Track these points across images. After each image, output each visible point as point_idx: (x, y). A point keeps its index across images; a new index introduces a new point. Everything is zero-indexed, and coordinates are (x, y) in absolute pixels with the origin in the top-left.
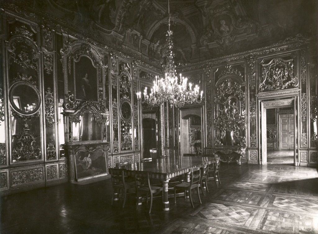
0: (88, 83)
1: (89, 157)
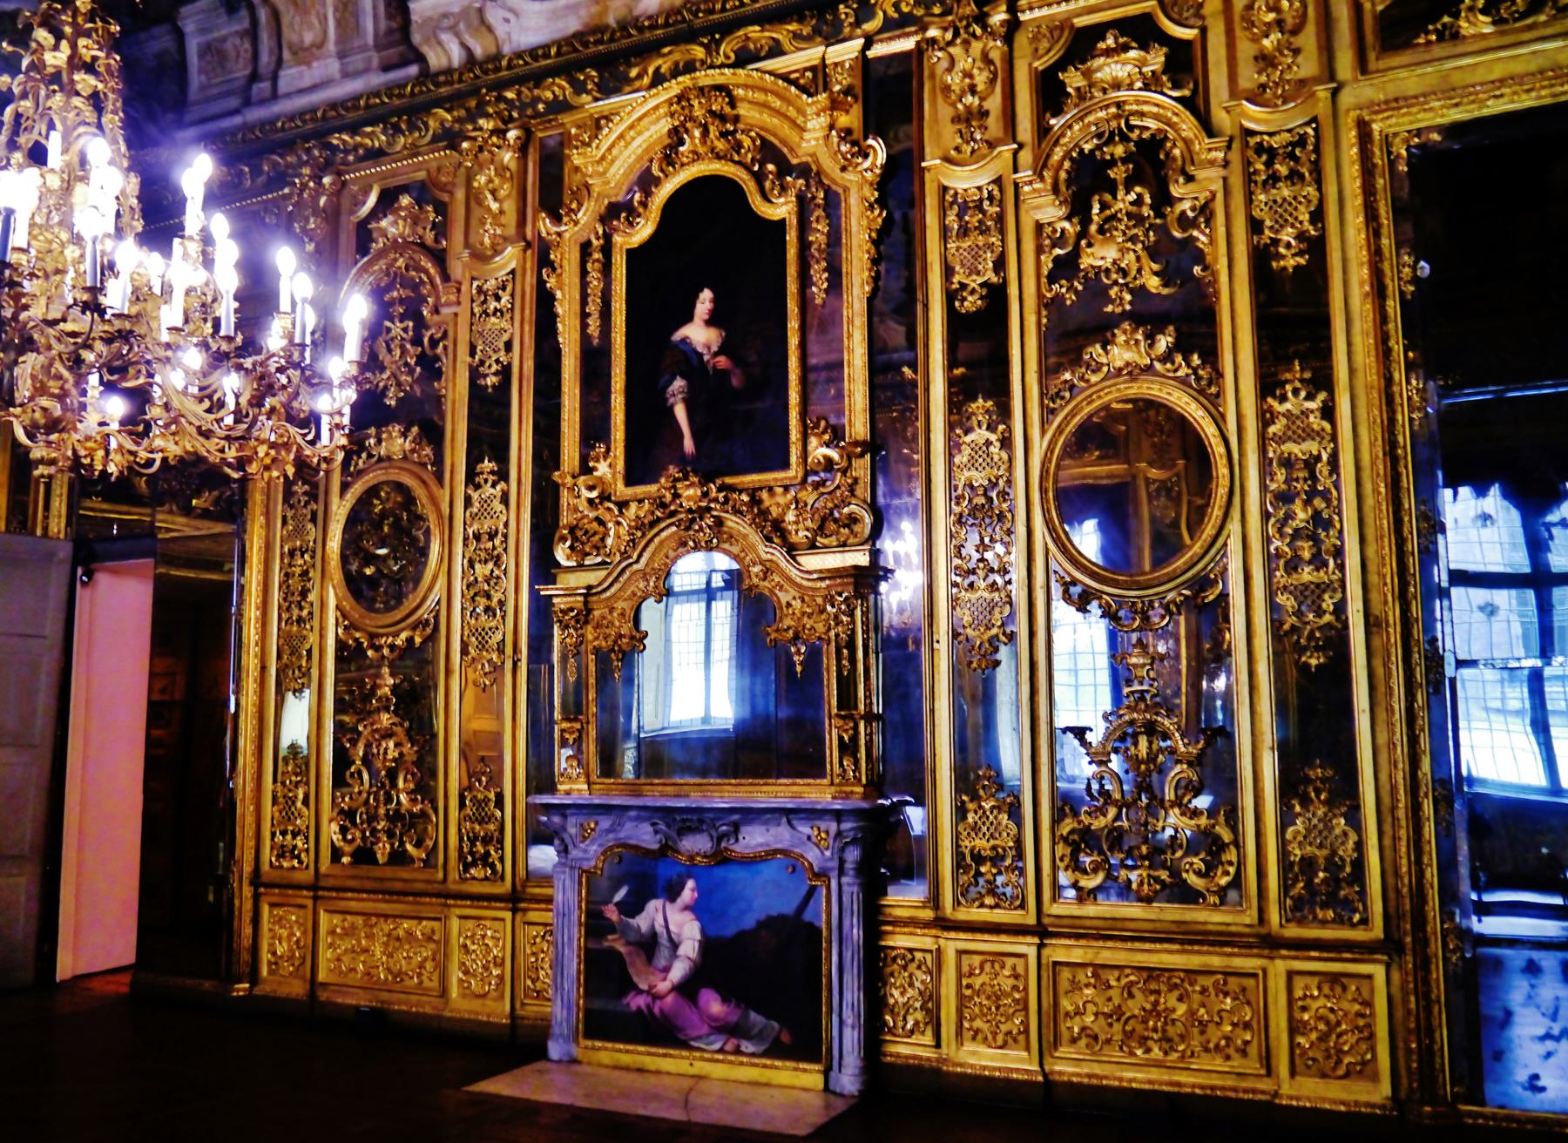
0: (715, 348)
1: (686, 908)
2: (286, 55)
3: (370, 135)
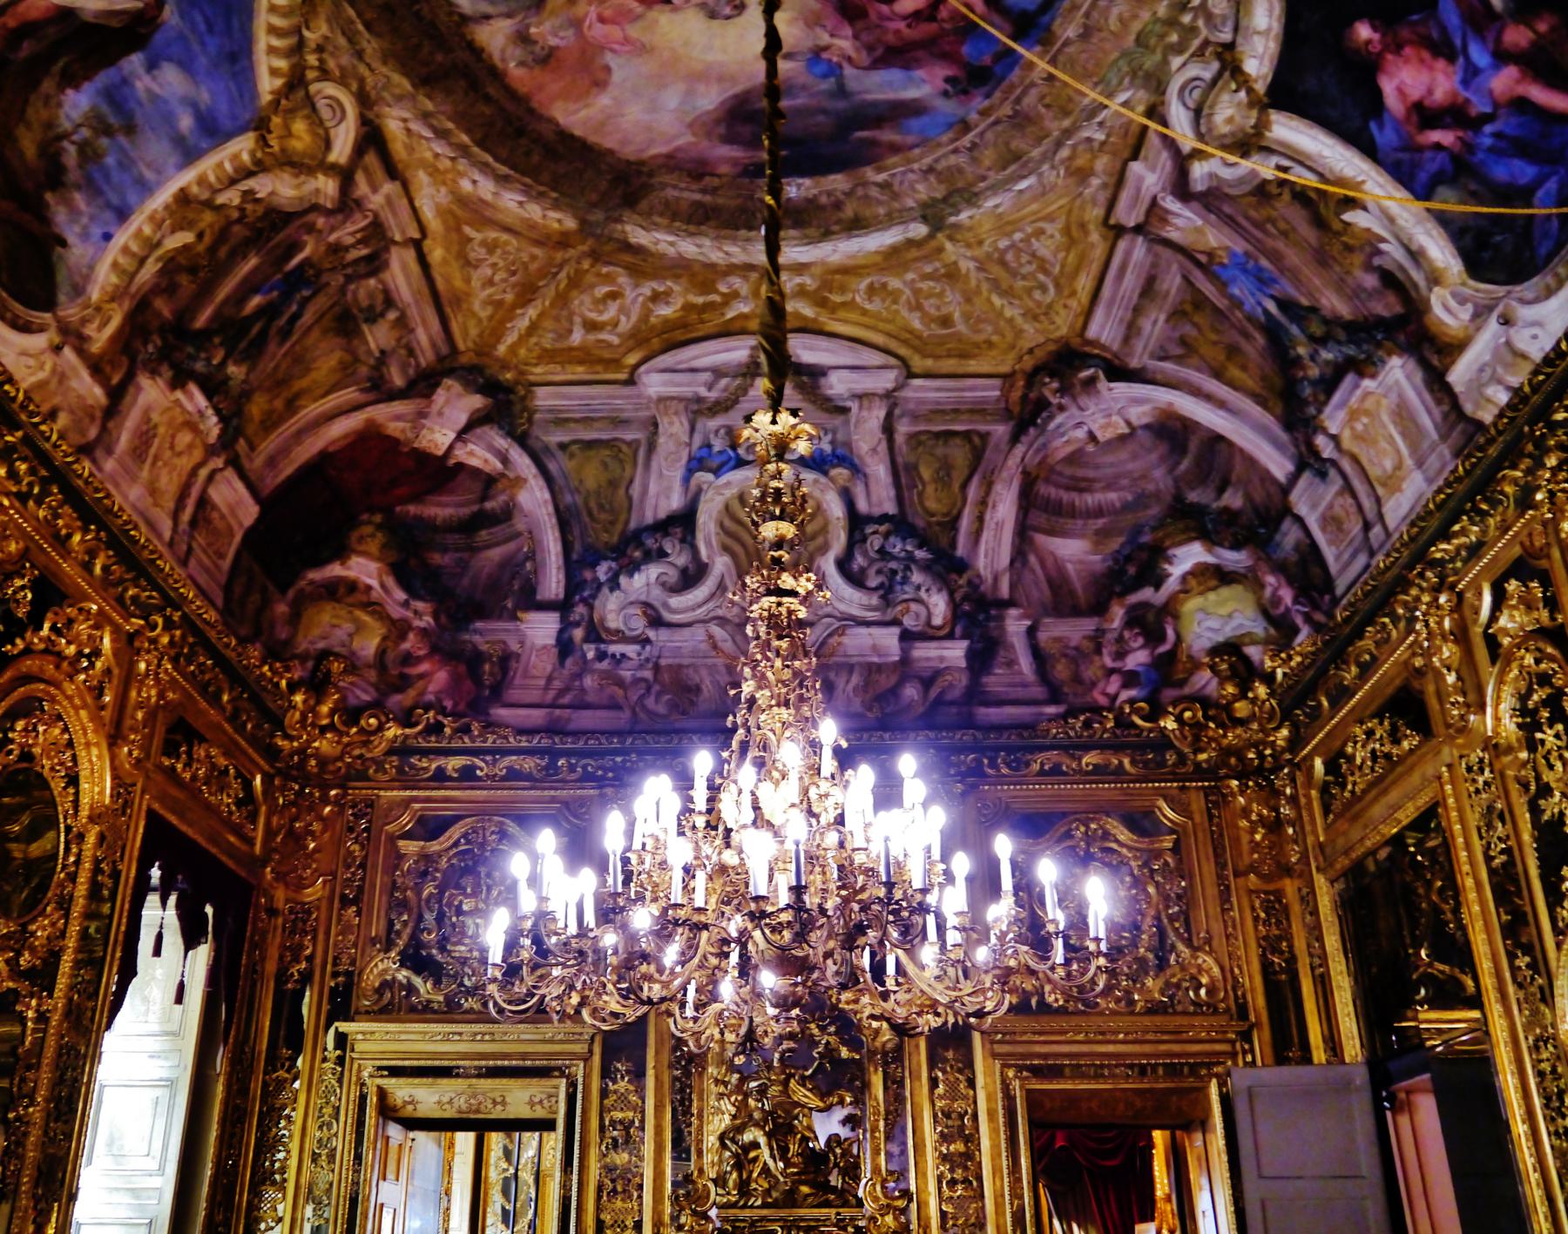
2: (1380, 491)
3: (1464, 532)
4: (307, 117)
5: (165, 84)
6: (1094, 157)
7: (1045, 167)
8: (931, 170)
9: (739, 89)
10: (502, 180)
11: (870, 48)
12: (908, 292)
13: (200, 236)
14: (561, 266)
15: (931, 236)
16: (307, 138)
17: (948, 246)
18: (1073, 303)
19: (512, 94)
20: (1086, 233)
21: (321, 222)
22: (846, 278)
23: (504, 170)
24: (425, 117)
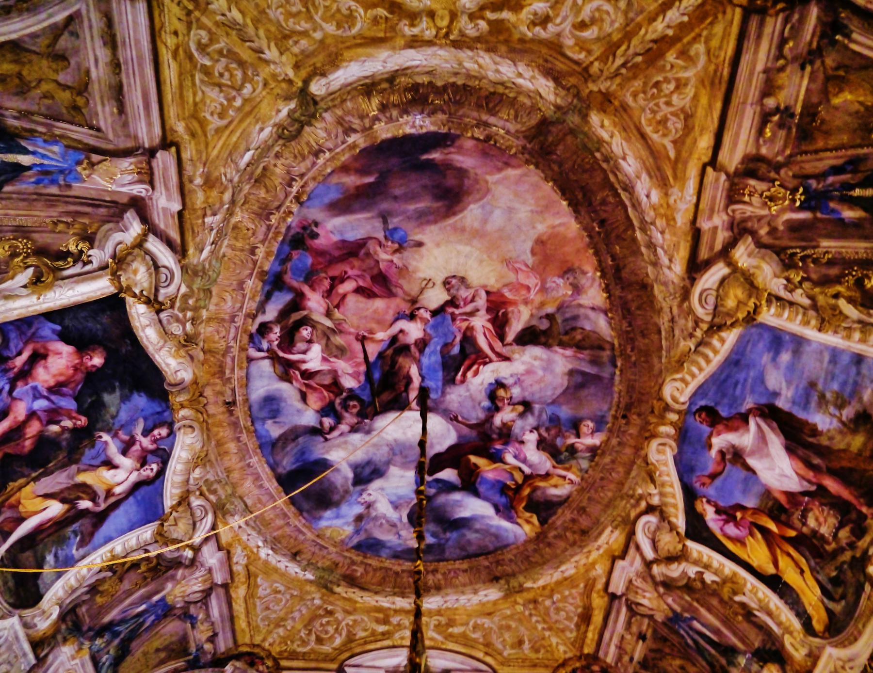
4: (722, 305)
5: (779, 382)
6: (206, 201)
7: (236, 179)
8: (317, 154)
9: (451, 221)
10: (629, 188)
11: (368, 254)
12: (317, 18)
13: (836, 296)
14: (617, 74)
15: (306, 82)
16: (731, 293)
17: (291, 73)
18: (171, 41)
19: (597, 253)
20: (188, 128)
21: (763, 232)
22: (372, 34)
23: (624, 196)
24: (656, 264)
